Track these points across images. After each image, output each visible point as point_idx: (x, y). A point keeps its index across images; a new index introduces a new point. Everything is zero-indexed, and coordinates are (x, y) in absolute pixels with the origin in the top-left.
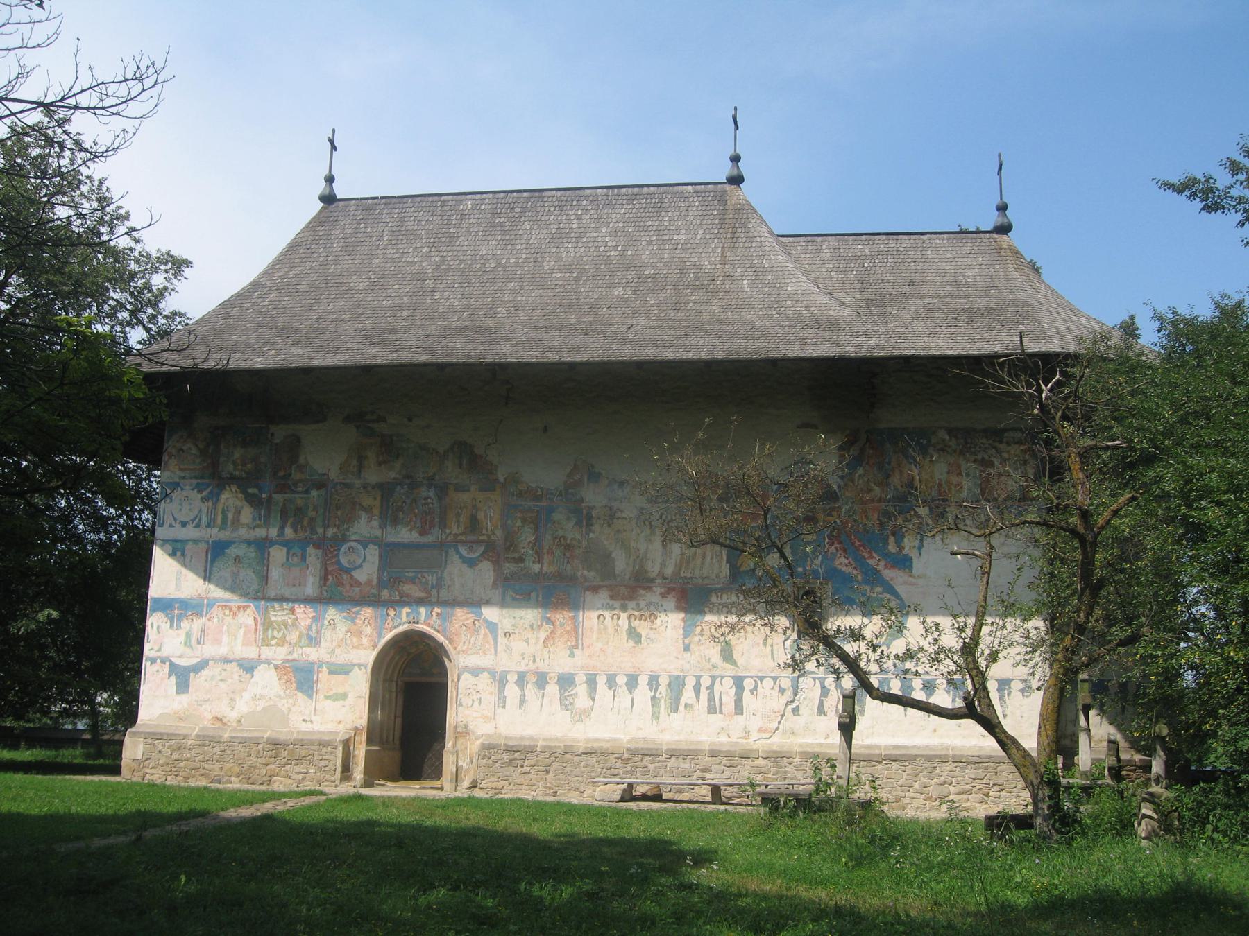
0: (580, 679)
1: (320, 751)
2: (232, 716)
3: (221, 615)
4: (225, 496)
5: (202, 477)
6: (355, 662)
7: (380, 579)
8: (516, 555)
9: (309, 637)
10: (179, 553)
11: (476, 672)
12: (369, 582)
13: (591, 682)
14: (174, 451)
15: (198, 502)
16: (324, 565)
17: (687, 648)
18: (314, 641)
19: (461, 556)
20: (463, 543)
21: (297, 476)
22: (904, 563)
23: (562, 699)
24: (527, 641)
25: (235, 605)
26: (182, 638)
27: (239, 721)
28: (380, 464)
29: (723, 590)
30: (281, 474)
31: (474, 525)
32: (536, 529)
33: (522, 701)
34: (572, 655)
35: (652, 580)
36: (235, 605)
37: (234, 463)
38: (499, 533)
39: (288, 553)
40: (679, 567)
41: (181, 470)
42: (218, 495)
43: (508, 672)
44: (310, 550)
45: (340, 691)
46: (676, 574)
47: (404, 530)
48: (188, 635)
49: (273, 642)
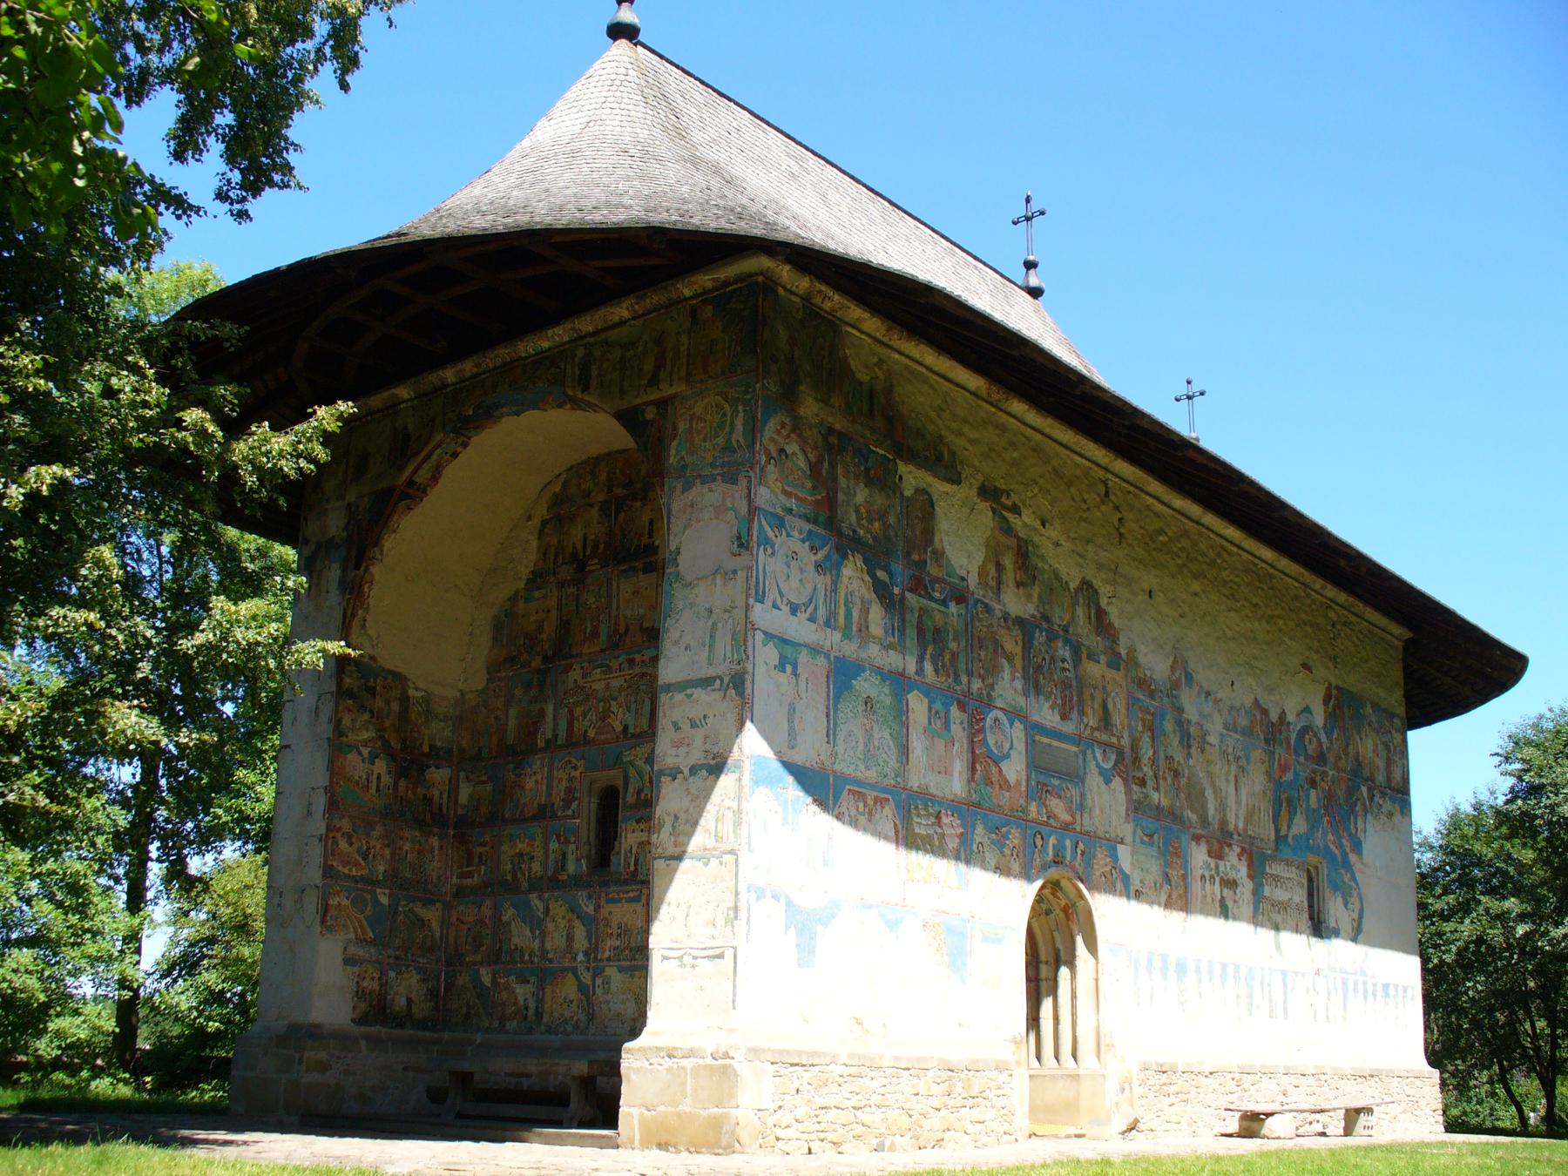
3: (853, 812)
5: (815, 522)
8: (1140, 775)
10: (789, 668)
12: (1019, 783)
13: (1198, 970)
14: (773, 449)
15: (811, 568)
19: (1098, 766)
21: (933, 570)
22: (1357, 847)
28: (1019, 584)
29: (1273, 858)
30: (915, 557)
35: (1231, 835)
37: (857, 510)
38: (1126, 742)
40: (1246, 824)
41: (785, 492)
42: (838, 567)
44: (954, 710)
46: (1245, 830)
47: (1047, 705)
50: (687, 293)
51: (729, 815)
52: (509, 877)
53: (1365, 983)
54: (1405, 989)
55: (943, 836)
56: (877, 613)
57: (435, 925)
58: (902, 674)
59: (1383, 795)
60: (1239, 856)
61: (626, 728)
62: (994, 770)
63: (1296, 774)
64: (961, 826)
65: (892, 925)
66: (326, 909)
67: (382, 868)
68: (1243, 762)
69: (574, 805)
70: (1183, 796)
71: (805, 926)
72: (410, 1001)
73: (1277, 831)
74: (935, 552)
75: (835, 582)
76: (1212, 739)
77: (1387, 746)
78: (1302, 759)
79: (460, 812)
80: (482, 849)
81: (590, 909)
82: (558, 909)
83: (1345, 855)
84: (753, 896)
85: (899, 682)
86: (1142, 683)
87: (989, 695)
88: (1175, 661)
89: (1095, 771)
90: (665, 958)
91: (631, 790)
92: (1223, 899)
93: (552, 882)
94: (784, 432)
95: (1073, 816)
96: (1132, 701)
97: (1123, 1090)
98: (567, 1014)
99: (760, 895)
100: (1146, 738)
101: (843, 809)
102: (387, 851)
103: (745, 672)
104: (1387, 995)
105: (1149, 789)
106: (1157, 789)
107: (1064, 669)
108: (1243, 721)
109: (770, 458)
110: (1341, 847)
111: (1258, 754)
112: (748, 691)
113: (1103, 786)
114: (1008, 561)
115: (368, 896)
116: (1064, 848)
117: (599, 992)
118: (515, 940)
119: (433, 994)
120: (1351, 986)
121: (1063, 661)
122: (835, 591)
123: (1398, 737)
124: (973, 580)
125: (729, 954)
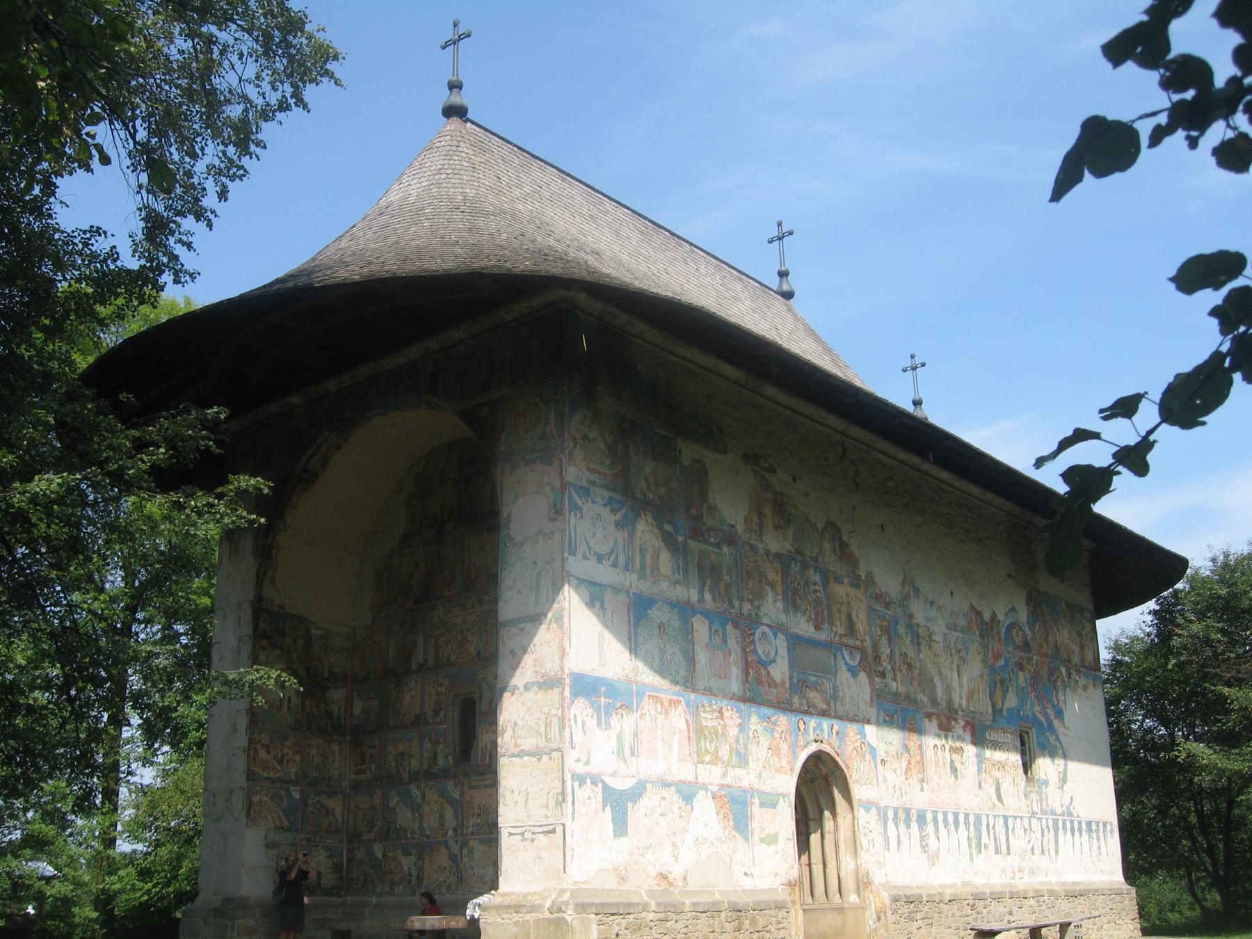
0: (929, 817)
1: (776, 917)
2: (676, 871)
3: (653, 713)
4: (641, 527)
5: (614, 490)
6: (780, 790)
7: (791, 679)
9: (738, 753)
11: (867, 805)
12: (783, 682)
13: (935, 820)
14: (578, 436)
15: (612, 528)
16: (744, 652)
17: (980, 787)
18: (743, 761)
19: (846, 664)
20: (847, 646)
21: (708, 521)
22: (1060, 714)
23: (922, 839)
24: (895, 771)
25: (666, 697)
26: (613, 745)
27: (685, 878)
28: (777, 527)
29: (991, 728)
30: (694, 512)
31: (851, 629)
32: (890, 640)
33: (899, 842)
34: (922, 790)
35: (956, 712)
36: (666, 697)
37: (647, 480)
38: (868, 644)
39: (710, 629)
40: (968, 701)
41: (589, 469)
42: (633, 523)
43: (887, 807)
44: (730, 628)
45: (772, 831)
46: (968, 706)
47: (804, 619)
48: (620, 737)
49: (707, 758)
50: (508, 317)
51: (555, 721)
52: (394, 772)
53: (1072, 822)
54: (1105, 825)
55: (725, 726)
56: (665, 558)
57: (338, 812)
58: (688, 603)
59: (1078, 671)
60: (964, 728)
61: (479, 653)
62: (763, 672)
63: (1007, 661)
64: (740, 717)
65: (688, 798)
66: (250, 806)
67: (293, 770)
68: (963, 654)
69: (442, 714)
70: (916, 683)
71: (619, 804)
72: (319, 874)
73: (994, 706)
74: (709, 507)
75: (631, 536)
76: (938, 637)
77: (1081, 636)
78: (1011, 649)
79: (355, 722)
80: (372, 751)
81: (457, 796)
82: (432, 796)
83: (1050, 722)
84: (576, 784)
85: (685, 610)
86: (879, 597)
87: (757, 614)
88: (905, 579)
89: (844, 668)
90: (510, 834)
91: (484, 701)
92: (952, 761)
93: (428, 775)
94: (587, 423)
95: (828, 704)
96: (872, 612)
97: (879, 918)
98: (442, 878)
99: (582, 783)
100: (884, 640)
101: (645, 711)
102: (298, 757)
103: (563, 609)
104: (1090, 830)
105: (889, 680)
106: (894, 679)
107: (815, 591)
108: (962, 622)
109: (576, 444)
110: (1046, 715)
111: (975, 646)
112: (566, 625)
113: (851, 679)
114: (768, 511)
115: (283, 793)
116: (822, 730)
117: (465, 860)
118: (400, 822)
119: (337, 868)
120: (1060, 824)
121: (815, 584)
122: (632, 542)
123: (1089, 626)
124: (740, 528)
125: (559, 829)
